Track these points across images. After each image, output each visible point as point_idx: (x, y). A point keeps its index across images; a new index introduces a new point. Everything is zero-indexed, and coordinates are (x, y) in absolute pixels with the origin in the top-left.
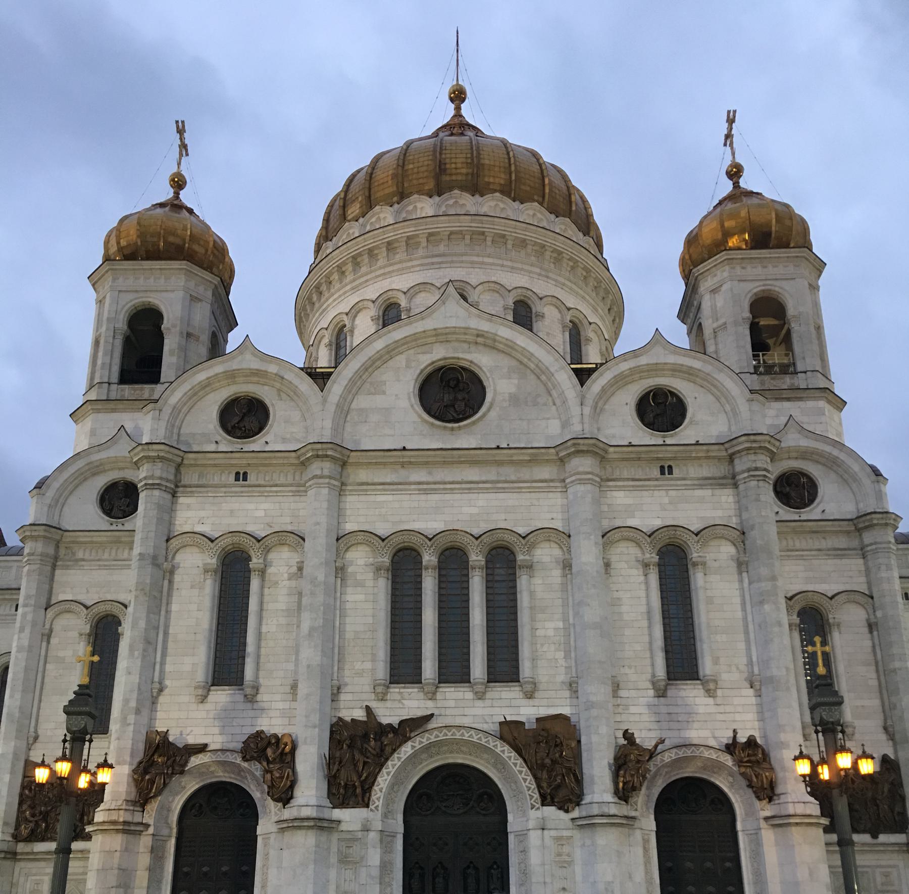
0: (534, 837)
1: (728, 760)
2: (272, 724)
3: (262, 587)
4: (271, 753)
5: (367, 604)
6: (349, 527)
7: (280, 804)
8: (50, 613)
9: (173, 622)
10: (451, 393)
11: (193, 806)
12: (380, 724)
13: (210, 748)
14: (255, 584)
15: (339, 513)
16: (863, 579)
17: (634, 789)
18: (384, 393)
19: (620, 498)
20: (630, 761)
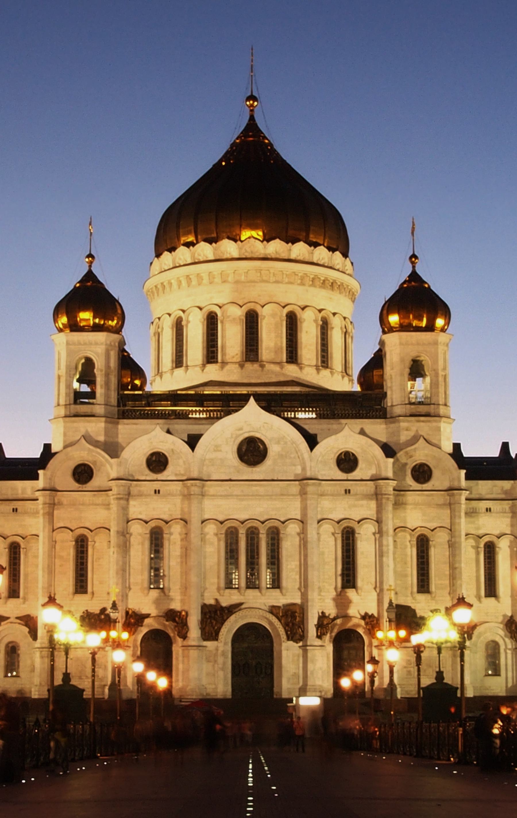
0: (284, 653)
1: (362, 623)
2: (176, 606)
3: (169, 545)
4: (177, 618)
5: (213, 551)
6: (206, 517)
7: (182, 639)
8: (54, 533)
9: (132, 560)
10: (252, 451)
11: (145, 638)
12: (222, 607)
13: (152, 615)
14: (166, 543)
15: (202, 510)
16: (449, 521)
17: (324, 634)
18: (221, 451)
19: (326, 503)
20: (324, 624)
